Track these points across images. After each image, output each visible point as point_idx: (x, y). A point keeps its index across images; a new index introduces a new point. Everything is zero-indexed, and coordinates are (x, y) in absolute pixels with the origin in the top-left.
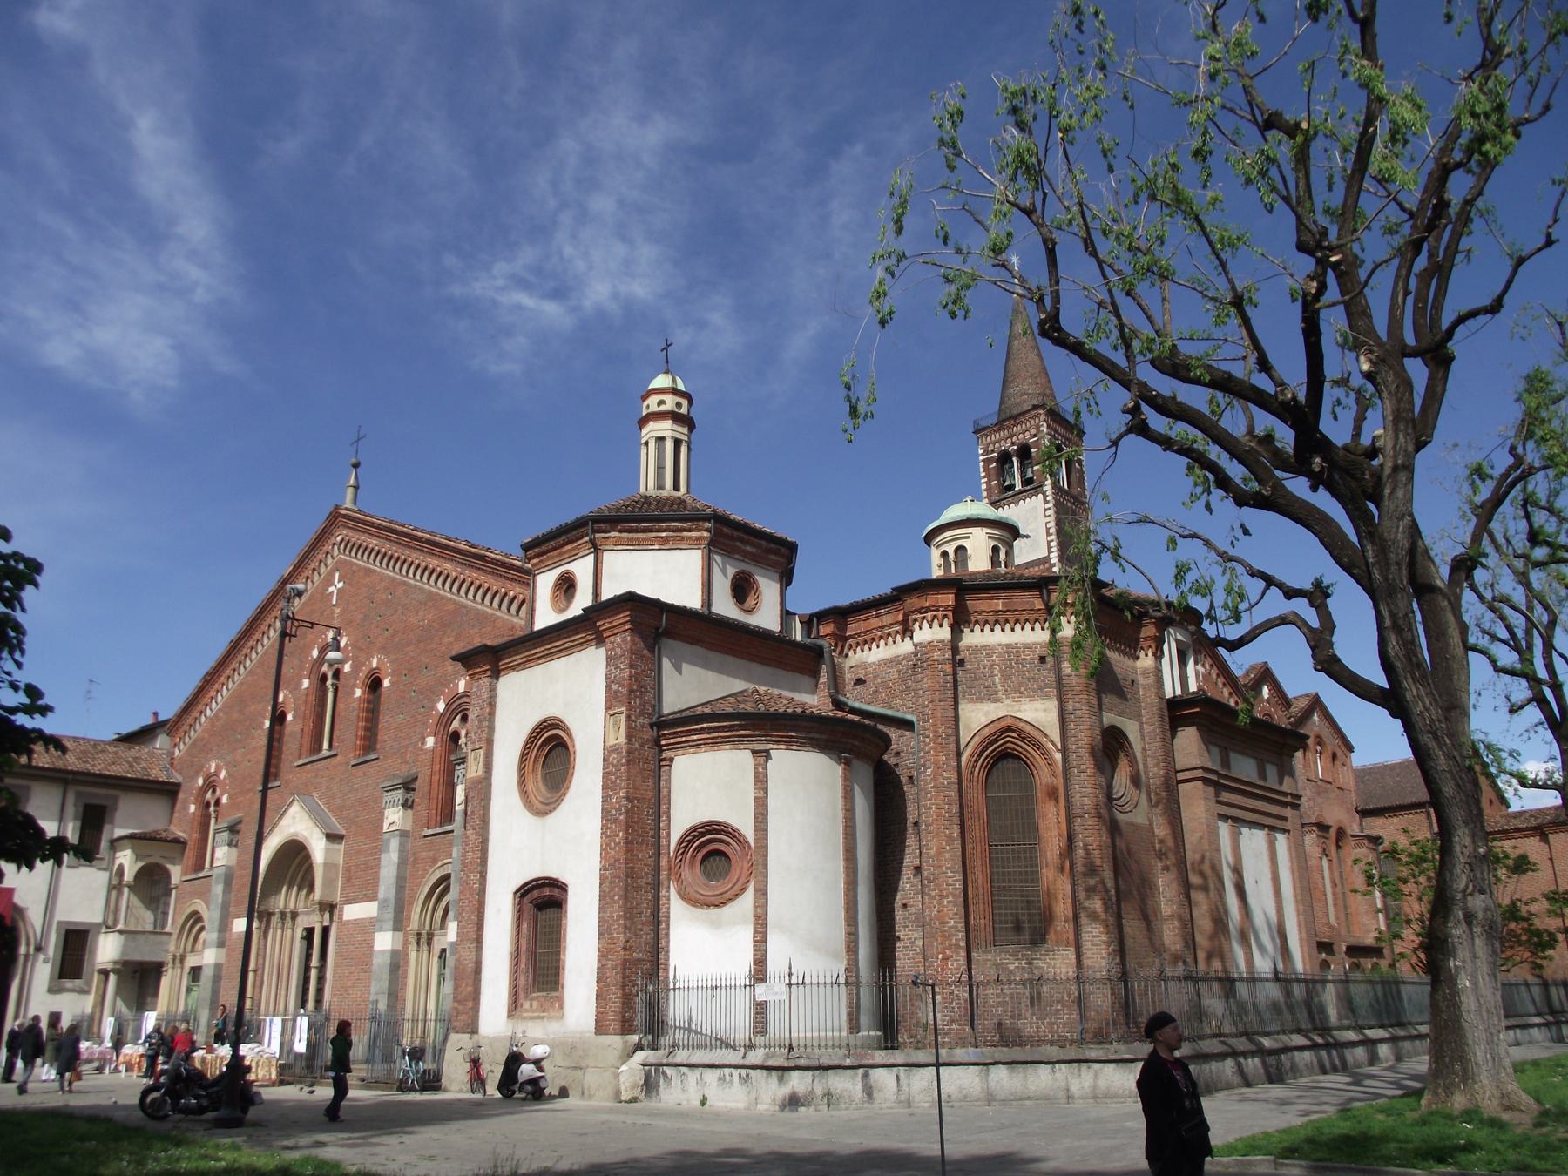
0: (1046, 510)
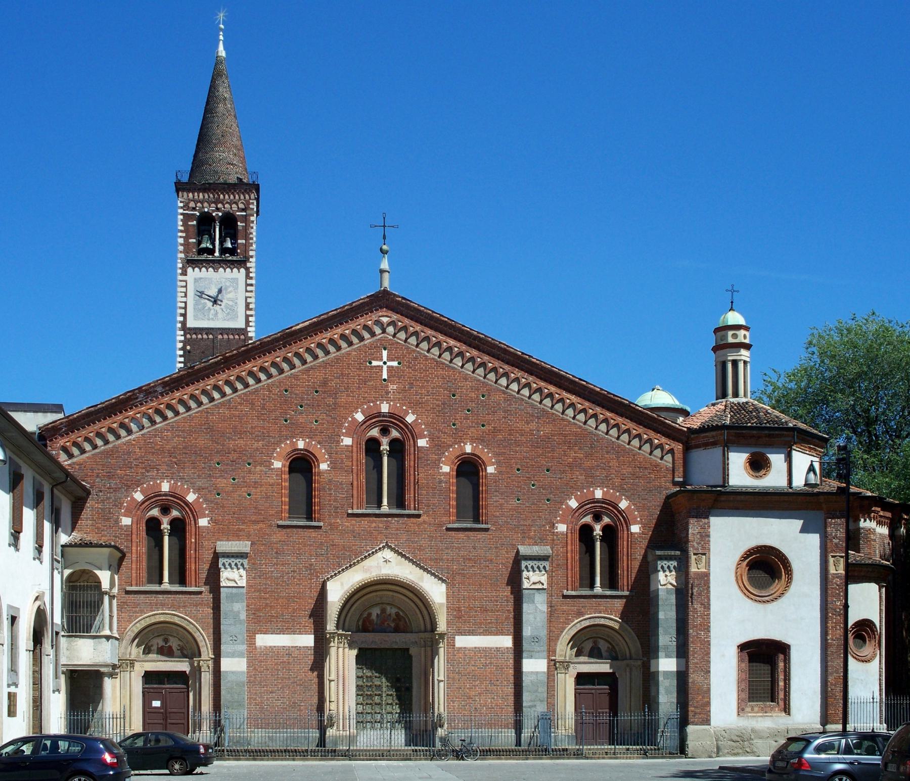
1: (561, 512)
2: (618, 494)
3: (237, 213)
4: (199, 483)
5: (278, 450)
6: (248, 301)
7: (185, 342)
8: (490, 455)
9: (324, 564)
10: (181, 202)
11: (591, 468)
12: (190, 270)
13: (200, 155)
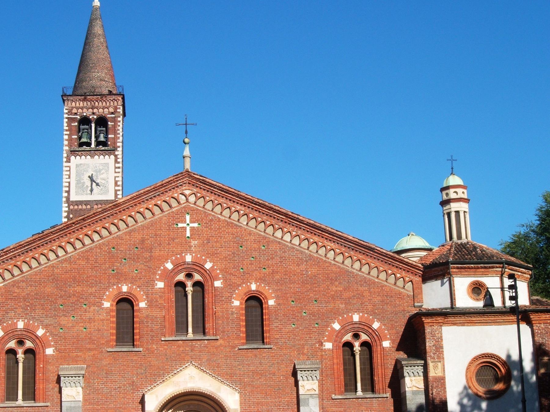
0: (116, 168)
1: (327, 333)
2: (371, 317)
3: (108, 116)
4: (46, 321)
5: (107, 293)
6: (116, 180)
7: (69, 212)
8: (270, 291)
9: (143, 381)
10: (66, 109)
11: (350, 298)
12: (73, 158)
13: (81, 75)
